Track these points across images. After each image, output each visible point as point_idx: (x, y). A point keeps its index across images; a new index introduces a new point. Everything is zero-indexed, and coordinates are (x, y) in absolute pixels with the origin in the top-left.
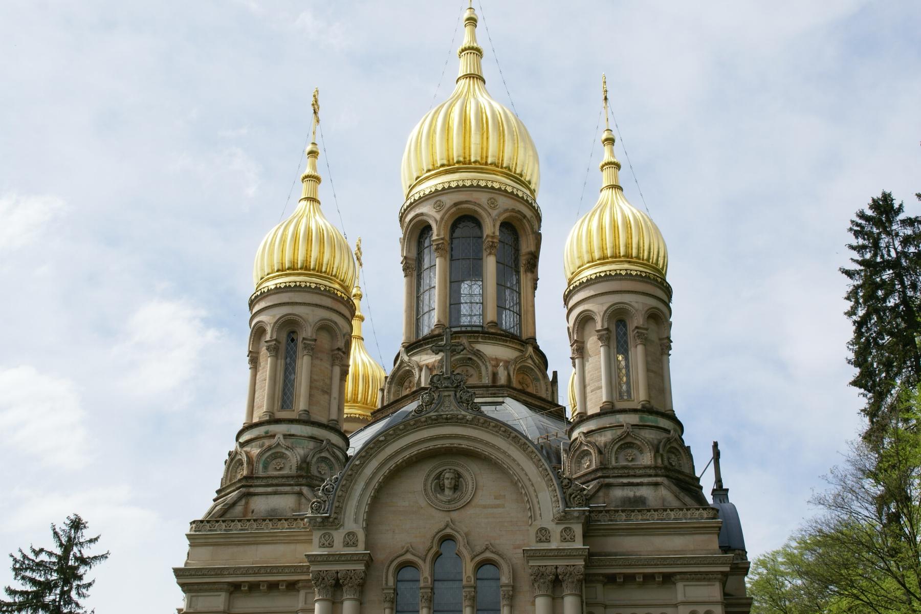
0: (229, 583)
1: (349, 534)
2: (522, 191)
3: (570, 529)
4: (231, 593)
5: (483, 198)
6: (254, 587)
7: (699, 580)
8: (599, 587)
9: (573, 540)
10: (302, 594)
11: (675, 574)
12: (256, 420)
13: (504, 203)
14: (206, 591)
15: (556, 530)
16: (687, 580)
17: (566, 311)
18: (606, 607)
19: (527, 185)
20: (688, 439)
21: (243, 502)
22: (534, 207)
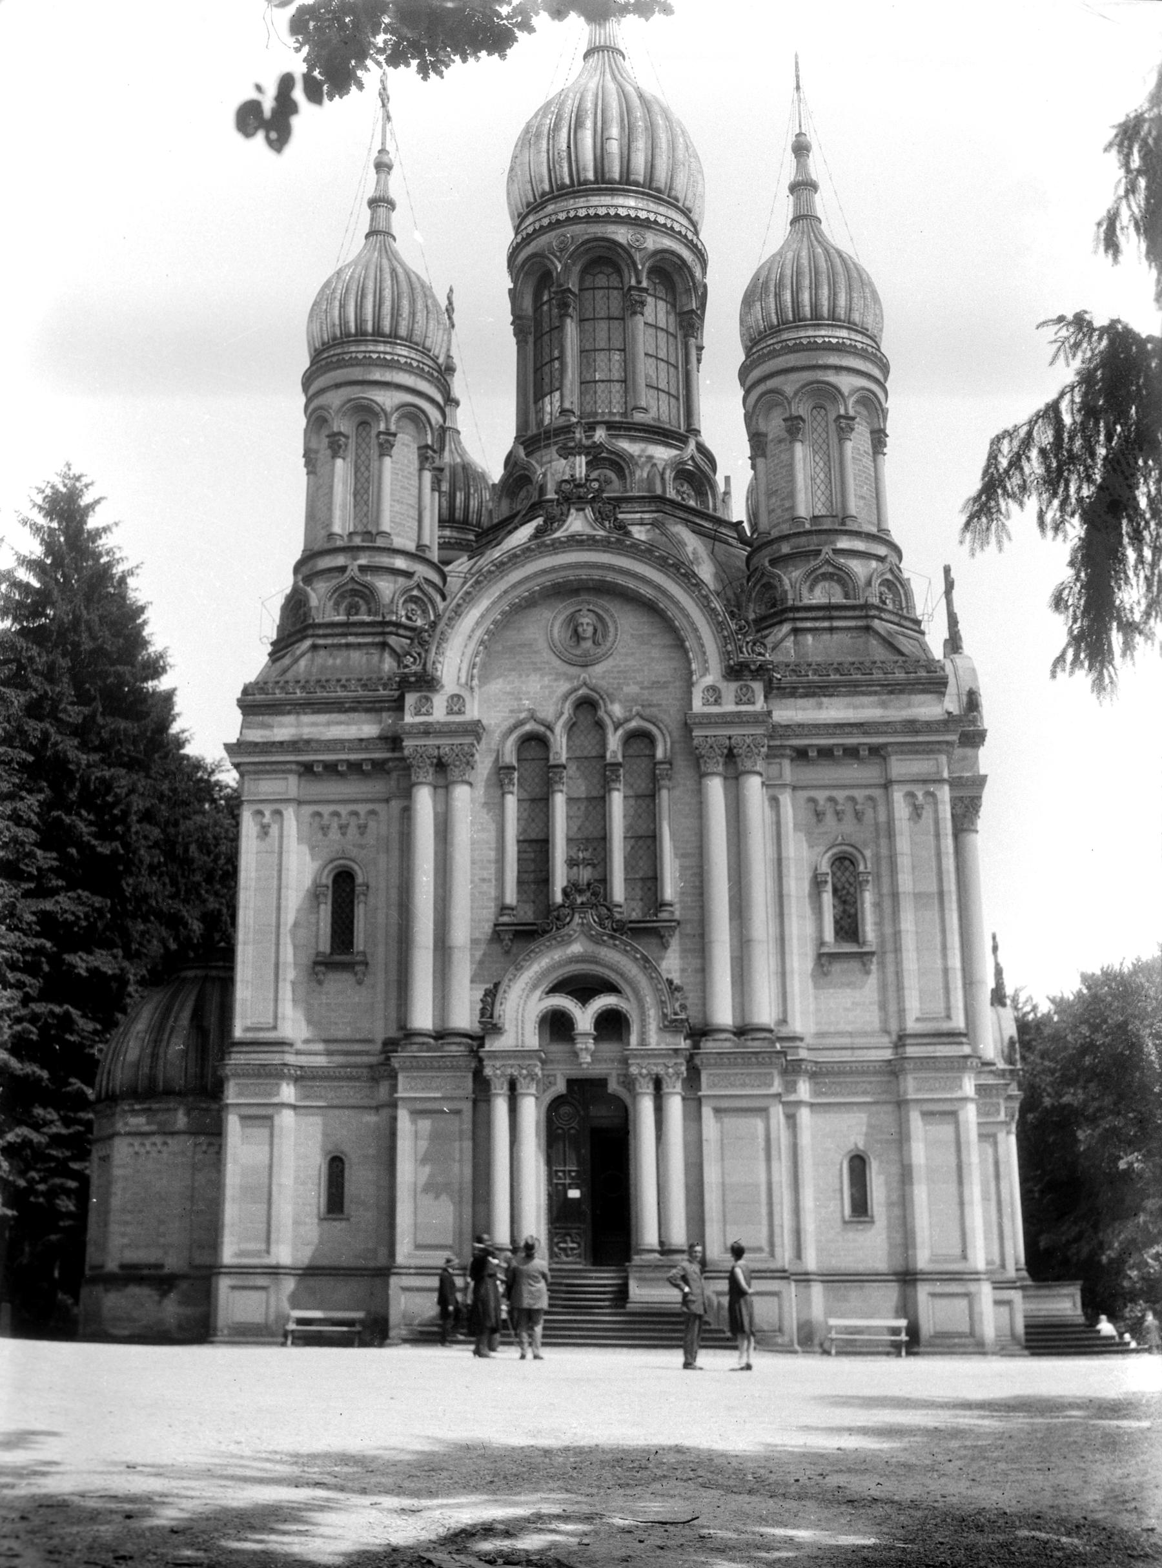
0: (298, 763)
1: (452, 697)
2: (680, 222)
3: (747, 687)
4: (300, 775)
5: (622, 235)
6: (331, 769)
7: (917, 752)
8: (786, 763)
9: (751, 702)
10: (394, 775)
11: (886, 745)
12: (317, 547)
13: (653, 241)
14: (268, 772)
15: (729, 690)
16: (902, 753)
17: (742, 393)
18: (794, 788)
19: (686, 212)
20: (909, 568)
21: (308, 656)
22: (696, 246)
